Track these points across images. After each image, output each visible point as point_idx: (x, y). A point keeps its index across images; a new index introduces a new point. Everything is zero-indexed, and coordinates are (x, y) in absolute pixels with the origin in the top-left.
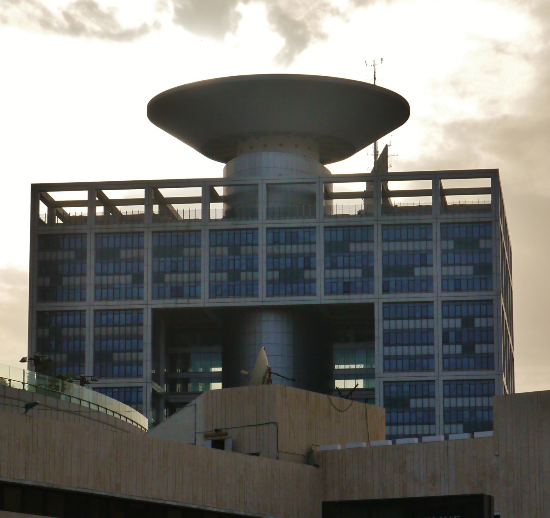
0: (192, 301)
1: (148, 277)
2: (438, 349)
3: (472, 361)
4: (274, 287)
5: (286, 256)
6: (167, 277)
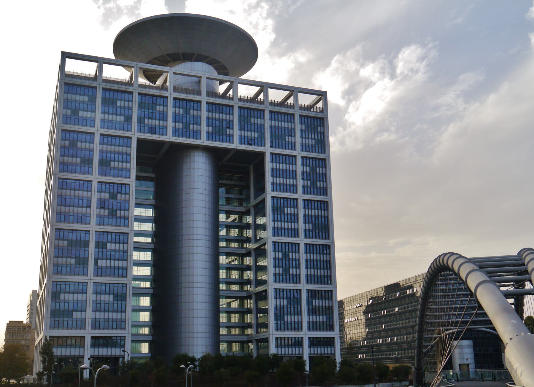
0: (161, 136)
1: (135, 119)
2: (300, 183)
4: (210, 136)
6: (146, 121)
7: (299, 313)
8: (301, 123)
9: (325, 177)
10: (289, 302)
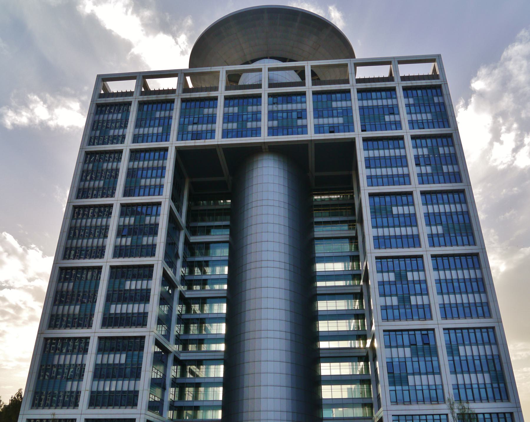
3: (441, 178)
4: (272, 131)
5: (282, 111)
7: (436, 371)
8: (406, 96)
10: (415, 353)
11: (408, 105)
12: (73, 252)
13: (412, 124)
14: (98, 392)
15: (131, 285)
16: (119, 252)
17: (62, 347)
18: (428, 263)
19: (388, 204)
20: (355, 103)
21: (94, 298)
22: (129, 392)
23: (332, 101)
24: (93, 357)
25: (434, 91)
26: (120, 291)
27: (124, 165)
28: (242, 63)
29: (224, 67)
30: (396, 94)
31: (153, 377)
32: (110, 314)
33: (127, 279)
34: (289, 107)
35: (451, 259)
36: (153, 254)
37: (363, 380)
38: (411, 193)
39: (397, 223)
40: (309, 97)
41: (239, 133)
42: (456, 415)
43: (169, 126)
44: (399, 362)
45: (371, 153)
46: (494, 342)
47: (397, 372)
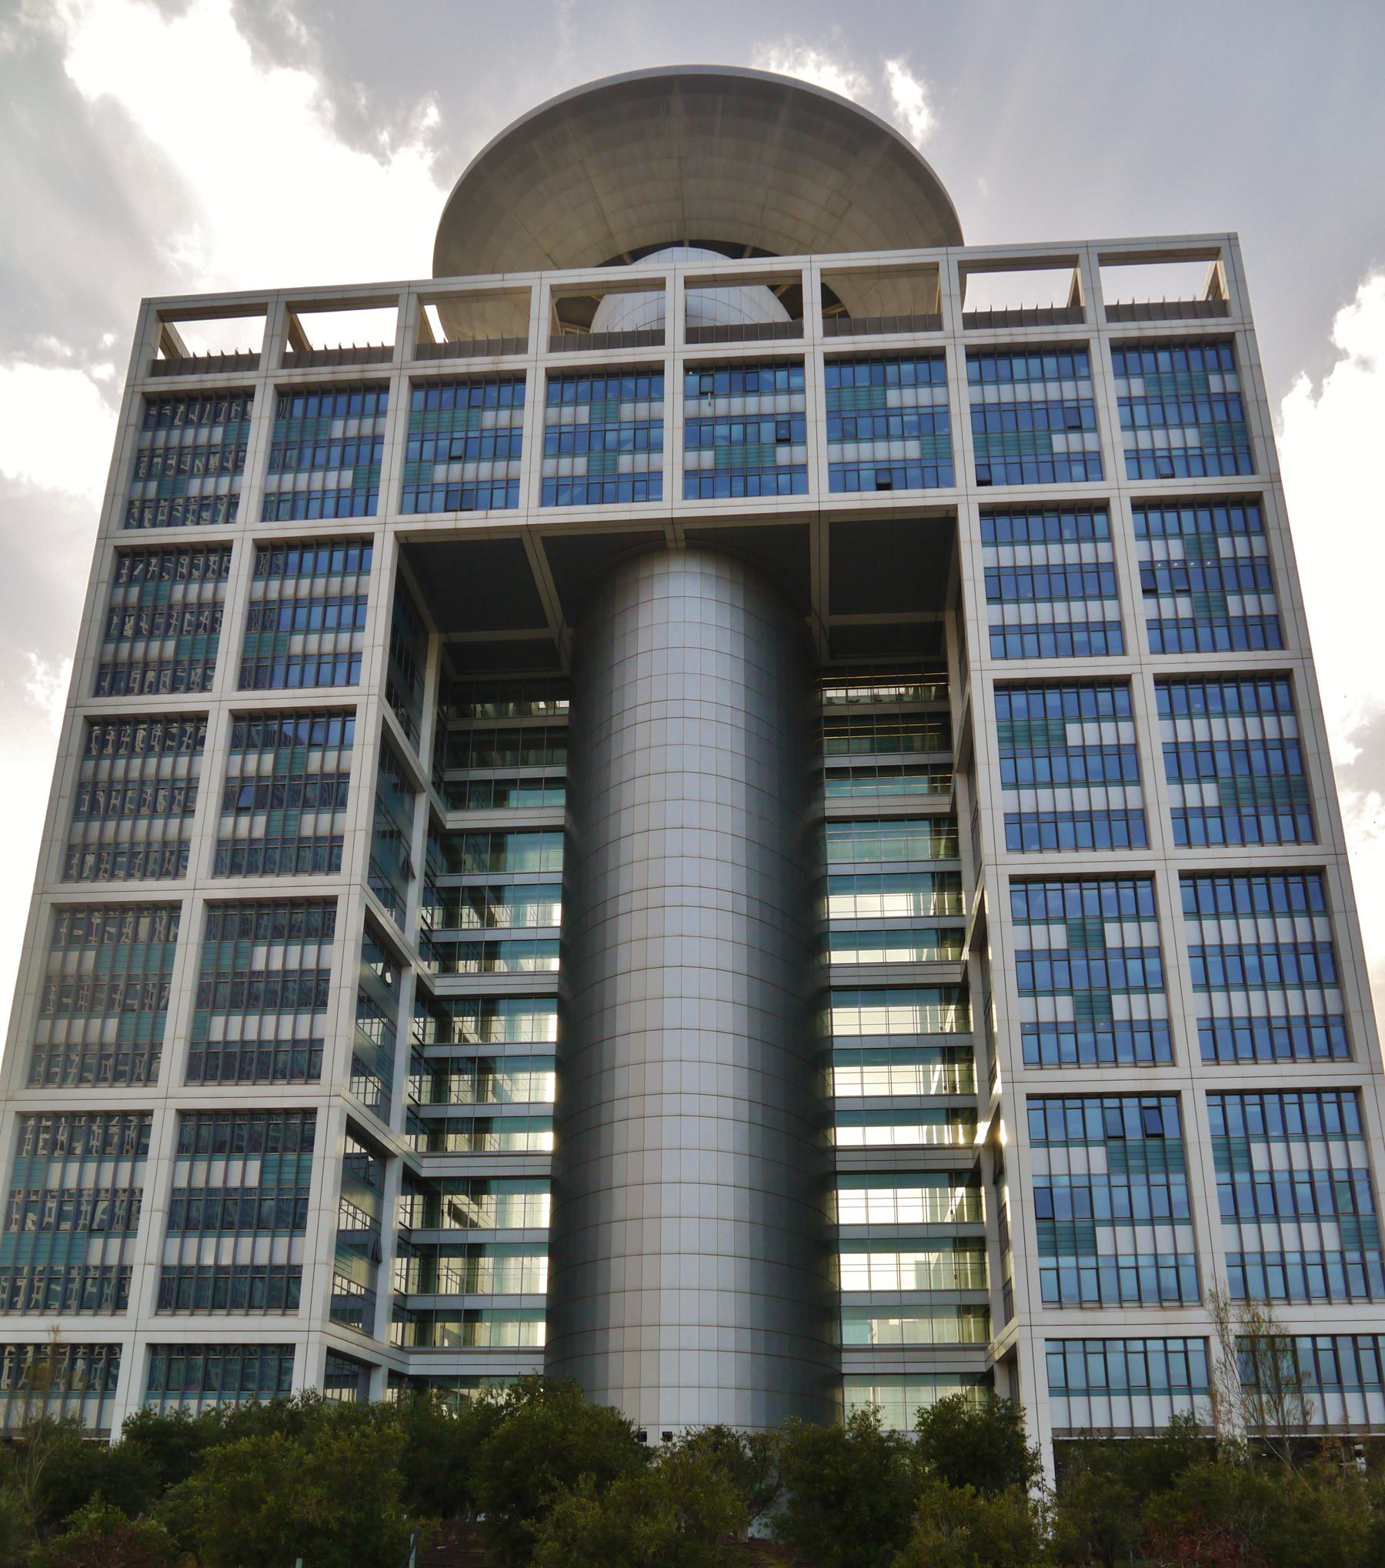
3: (1221, 633)
5: (729, 420)
7: (1179, 1215)
8: (1122, 372)
9: (1268, 572)
11: (1127, 402)
12: (90, 859)
13: (1137, 461)
14: (183, 1269)
15: (270, 958)
16: (233, 858)
17: (71, 1139)
18: (1171, 895)
19: (1054, 716)
20: (960, 394)
21: (160, 998)
22: (275, 1269)
23: (885, 385)
24: (165, 1166)
25: (1210, 354)
26: (236, 974)
27: (236, 591)
28: (602, 261)
29: (545, 274)
30: (1088, 364)
31: (343, 1227)
32: (210, 1044)
33: (256, 939)
34: (752, 404)
35: (1240, 885)
36: (333, 866)
37: (965, 1241)
38: (1124, 682)
39: (1078, 772)
40: (815, 374)
41: (595, 490)
42: (1232, 1339)
43: (374, 465)
44: (1071, 1187)
45: (1005, 556)
46: (1357, 1131)
47: (1063, 1216)
